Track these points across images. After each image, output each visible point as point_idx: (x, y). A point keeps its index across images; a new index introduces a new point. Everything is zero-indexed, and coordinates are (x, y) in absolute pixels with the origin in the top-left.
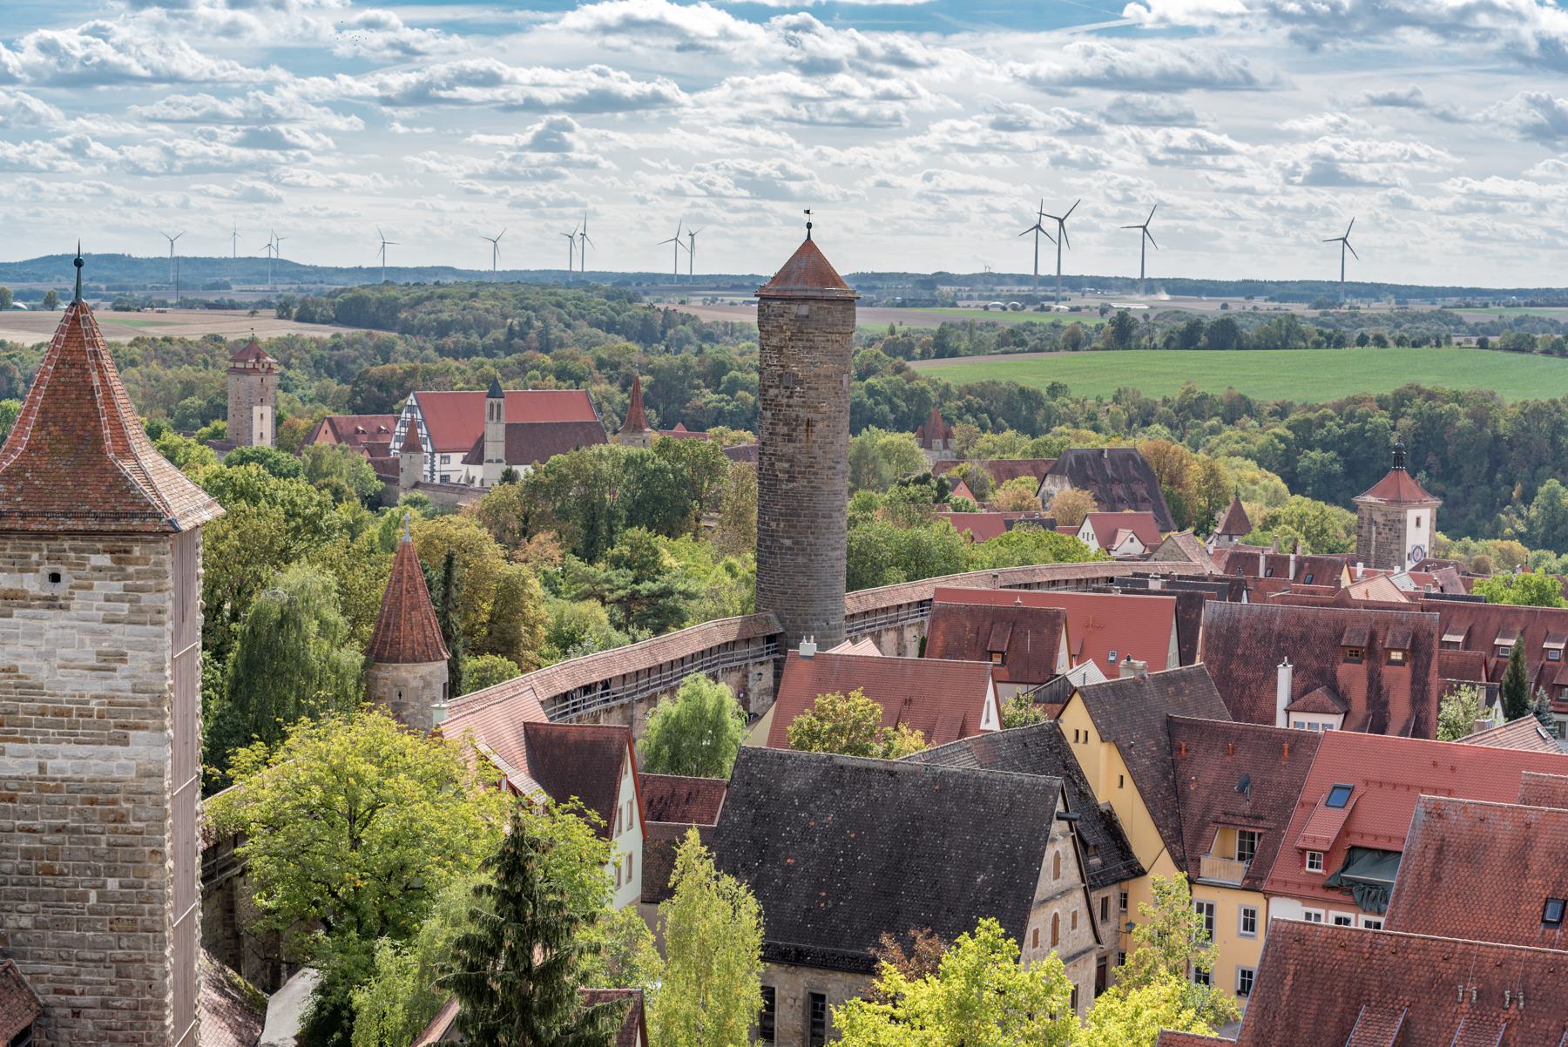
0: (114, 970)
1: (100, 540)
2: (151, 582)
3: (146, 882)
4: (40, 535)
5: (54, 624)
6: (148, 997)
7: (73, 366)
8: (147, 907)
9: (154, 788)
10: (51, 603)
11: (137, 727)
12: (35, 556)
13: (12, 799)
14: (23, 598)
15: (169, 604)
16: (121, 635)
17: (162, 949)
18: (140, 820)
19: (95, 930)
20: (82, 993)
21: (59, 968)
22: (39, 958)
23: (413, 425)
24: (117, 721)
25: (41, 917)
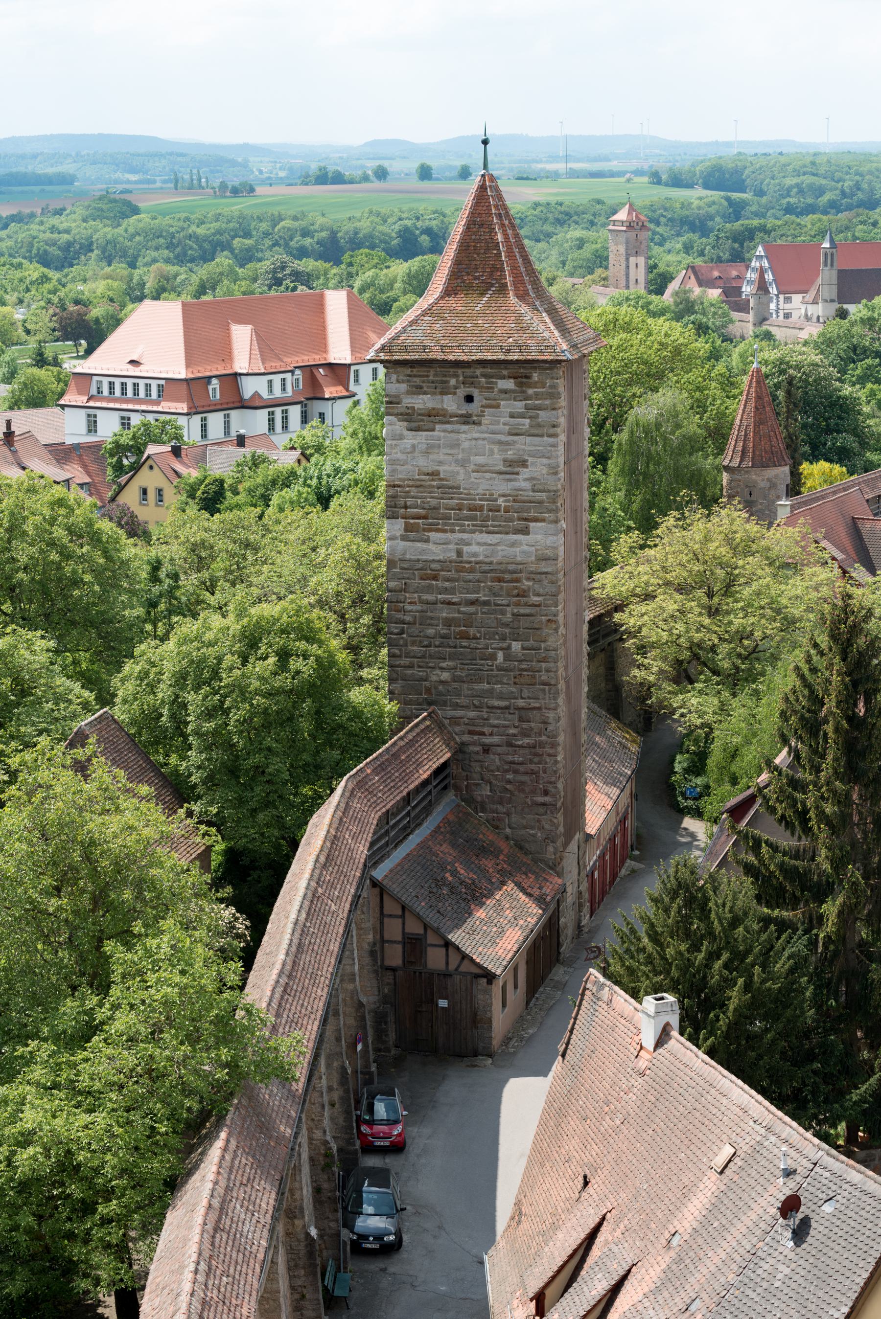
0: (516, 716)
1: (506, 368)
2: (547, 402)
3: (543, 645)
4: (458, 364)
5: (469, 436)
6: (544, 738)
7: (481, 225)
8: (544, 665)
9: (549, 570)
10: (466, 419)
11: (536, 520)
12: (453, 382)
13: (435, 578)
14: (444, 415)
15: (562, 420)
16: (524, 444)
17: (555, 699)
18: (538, 595)
19: (502, 683)
20: (491, 734)
21: (472, 714)
22: (456, 706)
23: (762, 272)
24: (520, 516)
25: (458, 673)
